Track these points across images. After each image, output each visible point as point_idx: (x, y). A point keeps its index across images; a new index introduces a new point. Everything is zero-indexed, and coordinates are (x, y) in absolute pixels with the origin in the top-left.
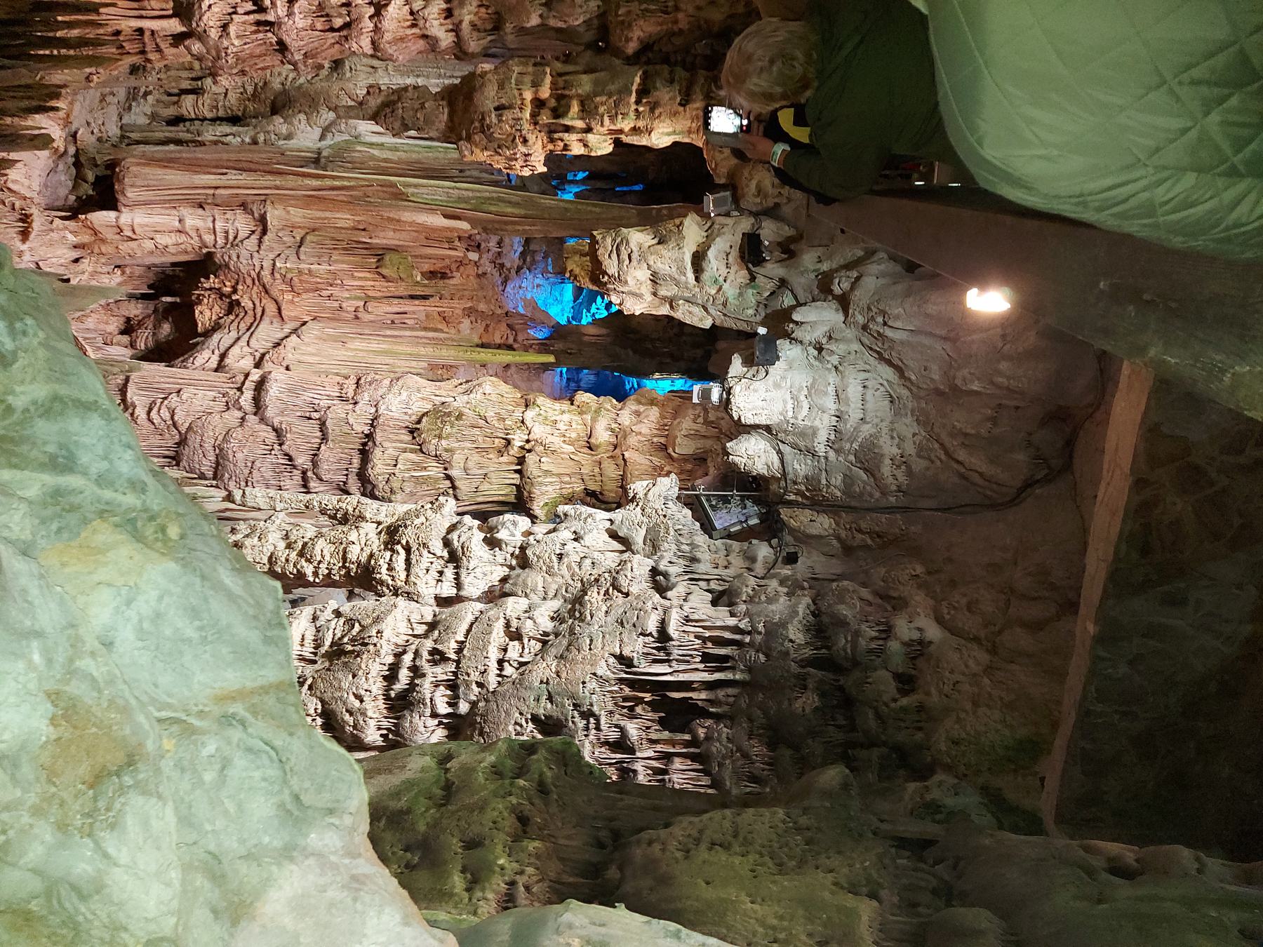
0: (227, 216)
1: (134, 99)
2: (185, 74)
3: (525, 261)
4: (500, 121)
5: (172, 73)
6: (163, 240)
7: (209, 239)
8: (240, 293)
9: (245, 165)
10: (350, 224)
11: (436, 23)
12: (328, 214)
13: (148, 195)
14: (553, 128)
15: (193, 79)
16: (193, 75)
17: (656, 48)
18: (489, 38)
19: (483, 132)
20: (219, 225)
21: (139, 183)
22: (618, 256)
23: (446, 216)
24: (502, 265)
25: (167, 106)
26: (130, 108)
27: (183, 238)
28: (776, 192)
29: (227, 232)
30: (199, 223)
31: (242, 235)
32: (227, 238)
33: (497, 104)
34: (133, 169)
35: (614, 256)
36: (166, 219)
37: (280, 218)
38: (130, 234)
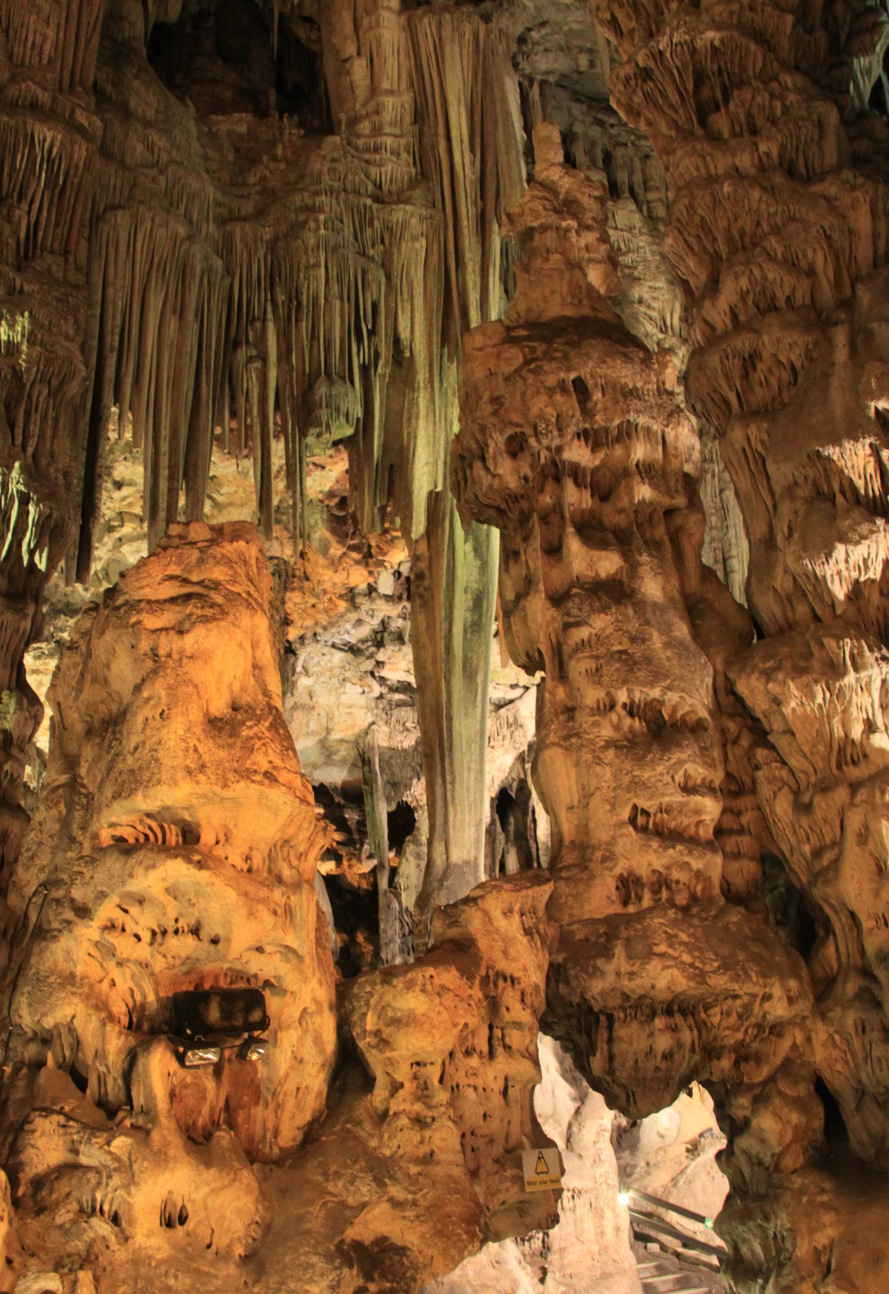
0: (404, 155)
1: (590, 108)
2: (638, 179)
3: (393, 690)
4: (551, 391)
5: (638, 164)
6: (359, 71)
7: (365, 127)
8: (272, 165)
9: (491, 185)
10: (404, 335)
11: (744, 283)
12: (419, 301)
13: (427, 45)
14: (554, 519)
15: (632, 190)
16: (640, 191)
17: (761, 754)
18: (732, 398)
19: (527, 363)
20: (389, 141)
21: (447, 31)
22: (173, 600)
23: (434, 499)
24: (380, 644)
25: (590, 152)
26: (578, 101)
27: (361, 92)
28: (403, 1074)
29: (377, 150)
30: (388, 116)
31: (374, 171)
32: (367, 150)
33: (590, 383)
34: (468, 30)
35: (171, 590)
36: (393, 69)
37: (405, 225)
38: (366, 22)
